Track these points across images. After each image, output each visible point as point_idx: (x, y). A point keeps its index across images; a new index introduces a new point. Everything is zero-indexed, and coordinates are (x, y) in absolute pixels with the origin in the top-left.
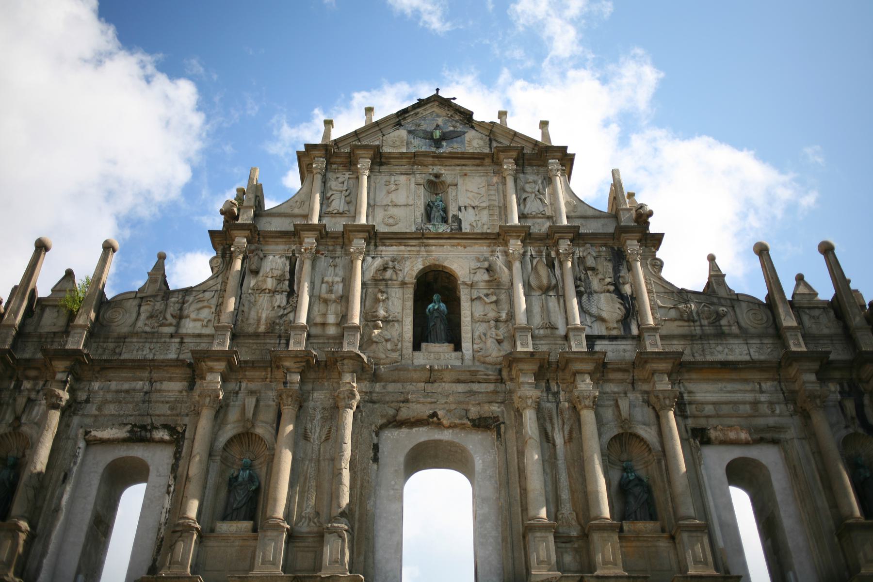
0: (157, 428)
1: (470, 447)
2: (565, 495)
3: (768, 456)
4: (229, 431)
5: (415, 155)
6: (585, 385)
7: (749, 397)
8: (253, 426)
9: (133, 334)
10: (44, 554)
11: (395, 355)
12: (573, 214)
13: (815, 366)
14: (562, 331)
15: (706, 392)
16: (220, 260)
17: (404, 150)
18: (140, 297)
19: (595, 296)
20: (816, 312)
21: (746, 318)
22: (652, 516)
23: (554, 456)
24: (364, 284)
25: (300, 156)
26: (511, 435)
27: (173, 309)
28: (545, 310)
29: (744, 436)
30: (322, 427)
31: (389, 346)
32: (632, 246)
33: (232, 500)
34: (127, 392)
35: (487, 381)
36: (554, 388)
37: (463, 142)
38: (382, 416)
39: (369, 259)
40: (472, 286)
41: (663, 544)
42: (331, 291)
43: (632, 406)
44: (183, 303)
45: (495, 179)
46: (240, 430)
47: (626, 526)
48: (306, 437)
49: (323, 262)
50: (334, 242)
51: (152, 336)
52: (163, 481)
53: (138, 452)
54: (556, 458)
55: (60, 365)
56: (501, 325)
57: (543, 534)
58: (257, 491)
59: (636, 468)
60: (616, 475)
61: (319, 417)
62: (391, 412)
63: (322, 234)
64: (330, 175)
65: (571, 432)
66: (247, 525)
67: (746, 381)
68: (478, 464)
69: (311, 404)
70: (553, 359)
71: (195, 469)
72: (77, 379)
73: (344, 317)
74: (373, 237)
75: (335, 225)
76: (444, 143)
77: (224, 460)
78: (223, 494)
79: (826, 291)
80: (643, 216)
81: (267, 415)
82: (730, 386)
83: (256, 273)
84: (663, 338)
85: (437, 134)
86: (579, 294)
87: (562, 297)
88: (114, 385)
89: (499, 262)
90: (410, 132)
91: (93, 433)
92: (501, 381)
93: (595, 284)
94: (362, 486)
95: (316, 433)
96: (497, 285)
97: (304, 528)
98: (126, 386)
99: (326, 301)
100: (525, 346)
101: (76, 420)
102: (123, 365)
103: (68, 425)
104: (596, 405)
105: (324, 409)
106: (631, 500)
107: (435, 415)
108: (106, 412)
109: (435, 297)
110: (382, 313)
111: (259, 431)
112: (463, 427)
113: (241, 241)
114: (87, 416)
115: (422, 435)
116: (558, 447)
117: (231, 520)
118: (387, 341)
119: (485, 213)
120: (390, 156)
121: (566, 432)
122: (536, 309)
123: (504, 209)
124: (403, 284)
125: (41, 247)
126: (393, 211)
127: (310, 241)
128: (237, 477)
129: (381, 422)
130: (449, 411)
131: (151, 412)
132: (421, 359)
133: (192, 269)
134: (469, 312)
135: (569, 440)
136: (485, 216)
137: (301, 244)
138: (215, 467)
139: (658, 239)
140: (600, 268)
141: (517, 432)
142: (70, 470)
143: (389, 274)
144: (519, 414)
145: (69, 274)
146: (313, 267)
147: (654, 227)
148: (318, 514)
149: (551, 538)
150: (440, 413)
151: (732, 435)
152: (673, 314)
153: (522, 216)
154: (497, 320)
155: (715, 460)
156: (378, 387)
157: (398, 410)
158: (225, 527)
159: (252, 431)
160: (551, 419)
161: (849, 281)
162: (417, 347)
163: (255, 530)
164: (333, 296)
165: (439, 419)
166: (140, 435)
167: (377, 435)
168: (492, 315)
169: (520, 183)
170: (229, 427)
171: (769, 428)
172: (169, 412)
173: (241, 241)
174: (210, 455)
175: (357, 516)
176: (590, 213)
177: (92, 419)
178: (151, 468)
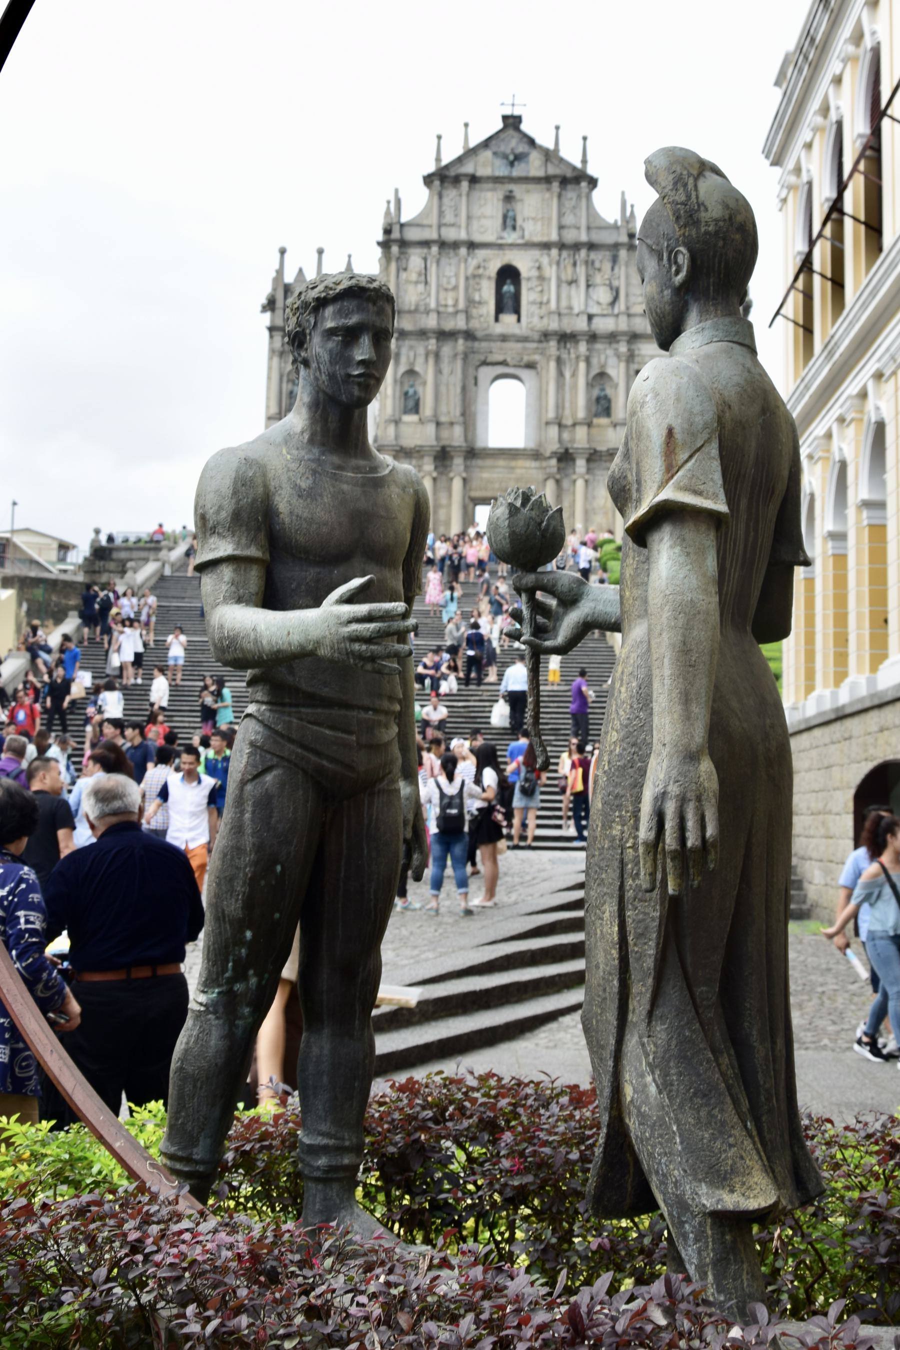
2: (567, 405)
4: (403, 369)
6: (583, 347)
11: (485, 325)
12: (592, 225)
14: (576, 311)
16: (384, 260)
19: (597, 288)
23: (564, 384)
24: (467, 278)
26: (544, 373)
28: (569, 298)
31: (482, 319)
32: (623, 253)
35: (533, 341)
36: (568, 345)
37: (527, 162)
39: (470, 259)
40: (529, 279)
42: (448, 283)
43: (607, 357)
45: (547, 195)
47: (596, 421)
49: (444, 261)
56: (544, 307)
60: (596, 392)
62: (482, 358)
63: (443, 244)
64: (445, 193)
70: (568, 331)
73: (456, 301)
74: (472, 246)
75: (450, 234)
76: (516, 163)
77: (402, 383)
83: (405, 269)
84: (629, 316)
85: (511, 157)
86: (588, 286)
87: (578, 287)
90: (495, 154)
92: (540, 341)
93: (598, 279)
97: (443, 419)
99: (446, 290)
100: (553, 325)
104: (588, 360)
109: (508, 281)
110: (477, 298)
112: (520, 366)
113: (395, 249)
115: (500, 370)
118: (481, 316)
119: (539, 223)
122: (564, 295)
123: (549, 225)
124: (489, 278)
125: (283, 252)
127: (435, 249)
134: (527, 297)
136: (539, 226)
137: (429, 248)
138: (398, 388)
140: (603, 268)
143: (481, 271)
145: (301, 270)
150: (509, 360)
153: (561, 227)
154: (541, 303)
156: (476, 344)
162: (497, 319)
164: (450, 287)
168: (539, 300)
169: (563, 198)
173: (395, 249)
174: (395, 381)
176: (603, 224)
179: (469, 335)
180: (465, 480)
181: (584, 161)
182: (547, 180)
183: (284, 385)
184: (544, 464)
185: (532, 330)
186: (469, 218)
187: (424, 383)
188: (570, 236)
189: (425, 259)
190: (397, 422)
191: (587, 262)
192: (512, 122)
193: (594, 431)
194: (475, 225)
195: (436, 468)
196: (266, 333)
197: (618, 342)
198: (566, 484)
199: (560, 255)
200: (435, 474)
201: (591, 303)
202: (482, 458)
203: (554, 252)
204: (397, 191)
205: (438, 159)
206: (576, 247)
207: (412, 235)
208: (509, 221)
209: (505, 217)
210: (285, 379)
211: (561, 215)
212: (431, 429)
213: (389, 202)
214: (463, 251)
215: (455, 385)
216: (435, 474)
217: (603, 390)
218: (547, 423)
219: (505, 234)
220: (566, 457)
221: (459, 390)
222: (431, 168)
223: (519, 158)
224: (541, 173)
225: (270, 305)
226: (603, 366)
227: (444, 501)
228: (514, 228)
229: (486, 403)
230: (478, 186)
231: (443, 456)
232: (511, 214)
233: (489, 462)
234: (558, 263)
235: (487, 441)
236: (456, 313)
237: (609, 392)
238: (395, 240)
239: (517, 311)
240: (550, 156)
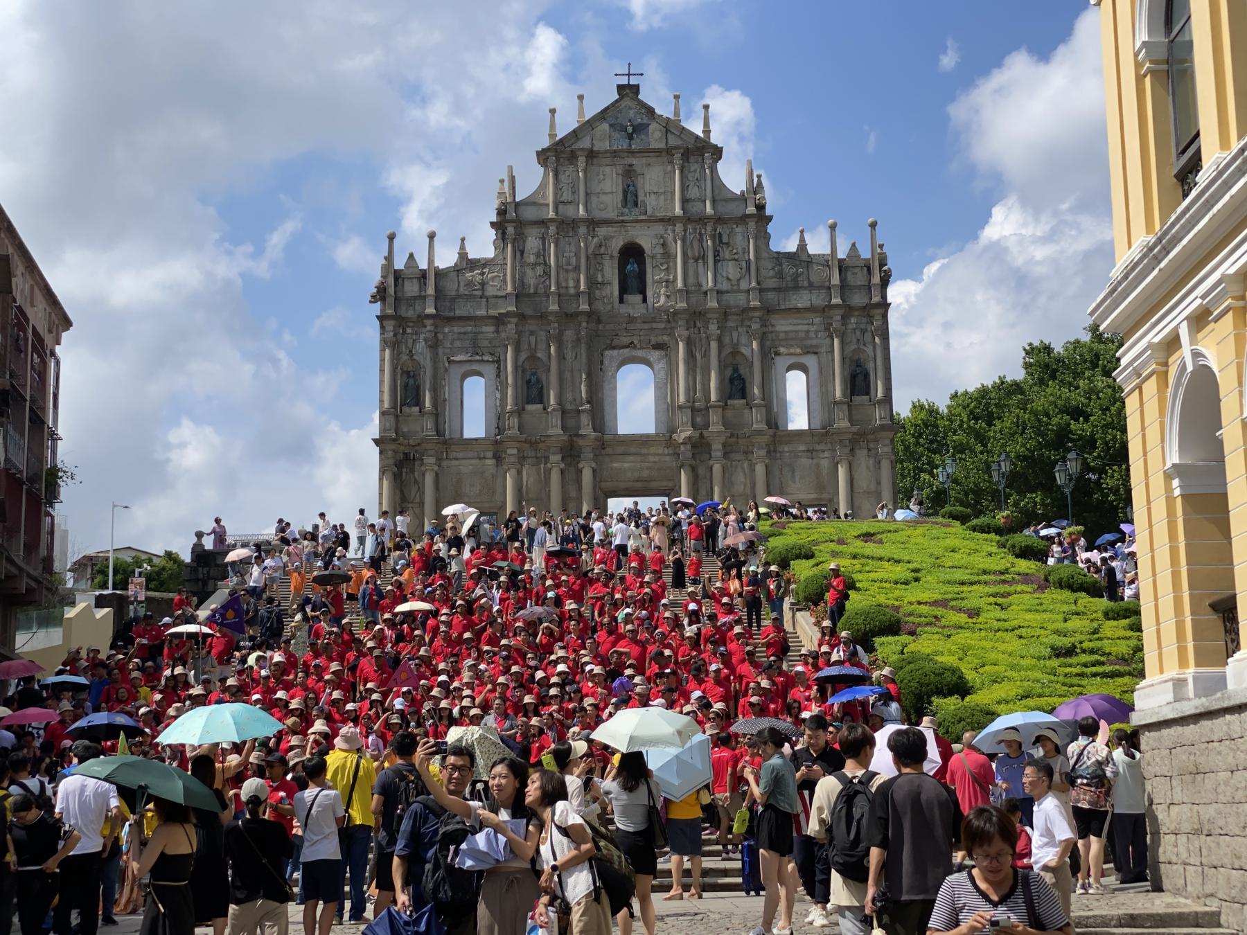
3: (811, 361)
4: (523, 356)
5: (615, 151)
6: (713, 328)
7: (806, 328)
9: (459, 296)
13: (841, 312)
14: (704, 288)
15: (782, 325)
16: (500, 242)
17: (606, 145)
18: (456, 270)
20: (857, 270)
21: (816, 275)
22: (744, 397)
24: (588, 258)
25: (538, 153)
27: (479, 278)
28: (697, 274)
29: (799, 351)
32: (752, 225)
34: (464, 333)
36: (698, 324)
37: (647, 135)
41: (747, 411)
42: (569, 264)
44: (483, 274)
45: (669, 168)
47: (729, 402)
49: (562, 242)
50: (567, 226)
51: (470, 297)
53: (476, 367)
55: (428, 322)
60: (729, 372)
64: (561, 169)
66: (540, 406)
67: (805, 318)
68: (656, 367)
69: (565, 338)
71: (510, 381)
72: (436, 327)
74: (592, 223)
77: (524, 371)
79: (865, 253)
80: (761, 208)
81: (542, 346)
82: (795, 322)
84: (761, 291)
85: (630, 130)
86: (716, 262)
88: (456, 329)
89: (670, 238)
90: (611, 126)
92: (669, 322)
95: (570, 355)
96: (668, 256)
97: (569, 407)
98: (463, 330)
99: (567, 271)
101: (440, 351)
102: (460, 318)
110: (600, 279)
111: (539, 355)
113: (510, 230)
115: (626, 352)
120: (598, 152)
126: (603, 198)
132: (624, 309)
133: (483, 245)
136: (662, 202)
139: (770, 218)
143: (602, 250)
145: (411, 255)
146: (556, 246)
147: (768, 212)
151: (792, 351)
152: (771, 273)
153: (685, 201)
155: (781, 363)
156: (601, 327)
161: (881, 246)
162: (621, 301)
171: (812, 346)
176: (729, 196)
179: (592, 315)
180: (594, 471)
181: (707, 132)
182: (669, 152)
185: (659, 309)
186: (587, 194)
187: (549, 370)
188: (695, 208)
189: (543, 239)
191: (713, 237)
192: (628, 91)
193: (729, 413)
194: (594, 201)
196: (377, 323)
197: (751, 319)
198: (702, 471)
199: (685, 230)
200: (562, 466)
201: (719, 278)
203: (679, 227)
204: (510, 168)
205: (552, 136)
206: (702, 220)
207: (529, 214)
208: (630, 197)
209: (625, 192)
211: (684, 188)
213: (502, 181)
214: (583, 230)
216: (562, 466)
217: (736, 370)
219: (626, 210)
222: (546, 143)
223: (639, 129)
224: (662, 146)
225: (381, 294)
226: (735, 346)
227: (573, 494)
228: (636, 204)
230: (595, 161)
232: (631, 188)
233: (619, 449)
234: (684, 240)
236: (578, 294)
237: (742, 371)
238: (511, 221)
239: (643, 292)
240: (671, 127)
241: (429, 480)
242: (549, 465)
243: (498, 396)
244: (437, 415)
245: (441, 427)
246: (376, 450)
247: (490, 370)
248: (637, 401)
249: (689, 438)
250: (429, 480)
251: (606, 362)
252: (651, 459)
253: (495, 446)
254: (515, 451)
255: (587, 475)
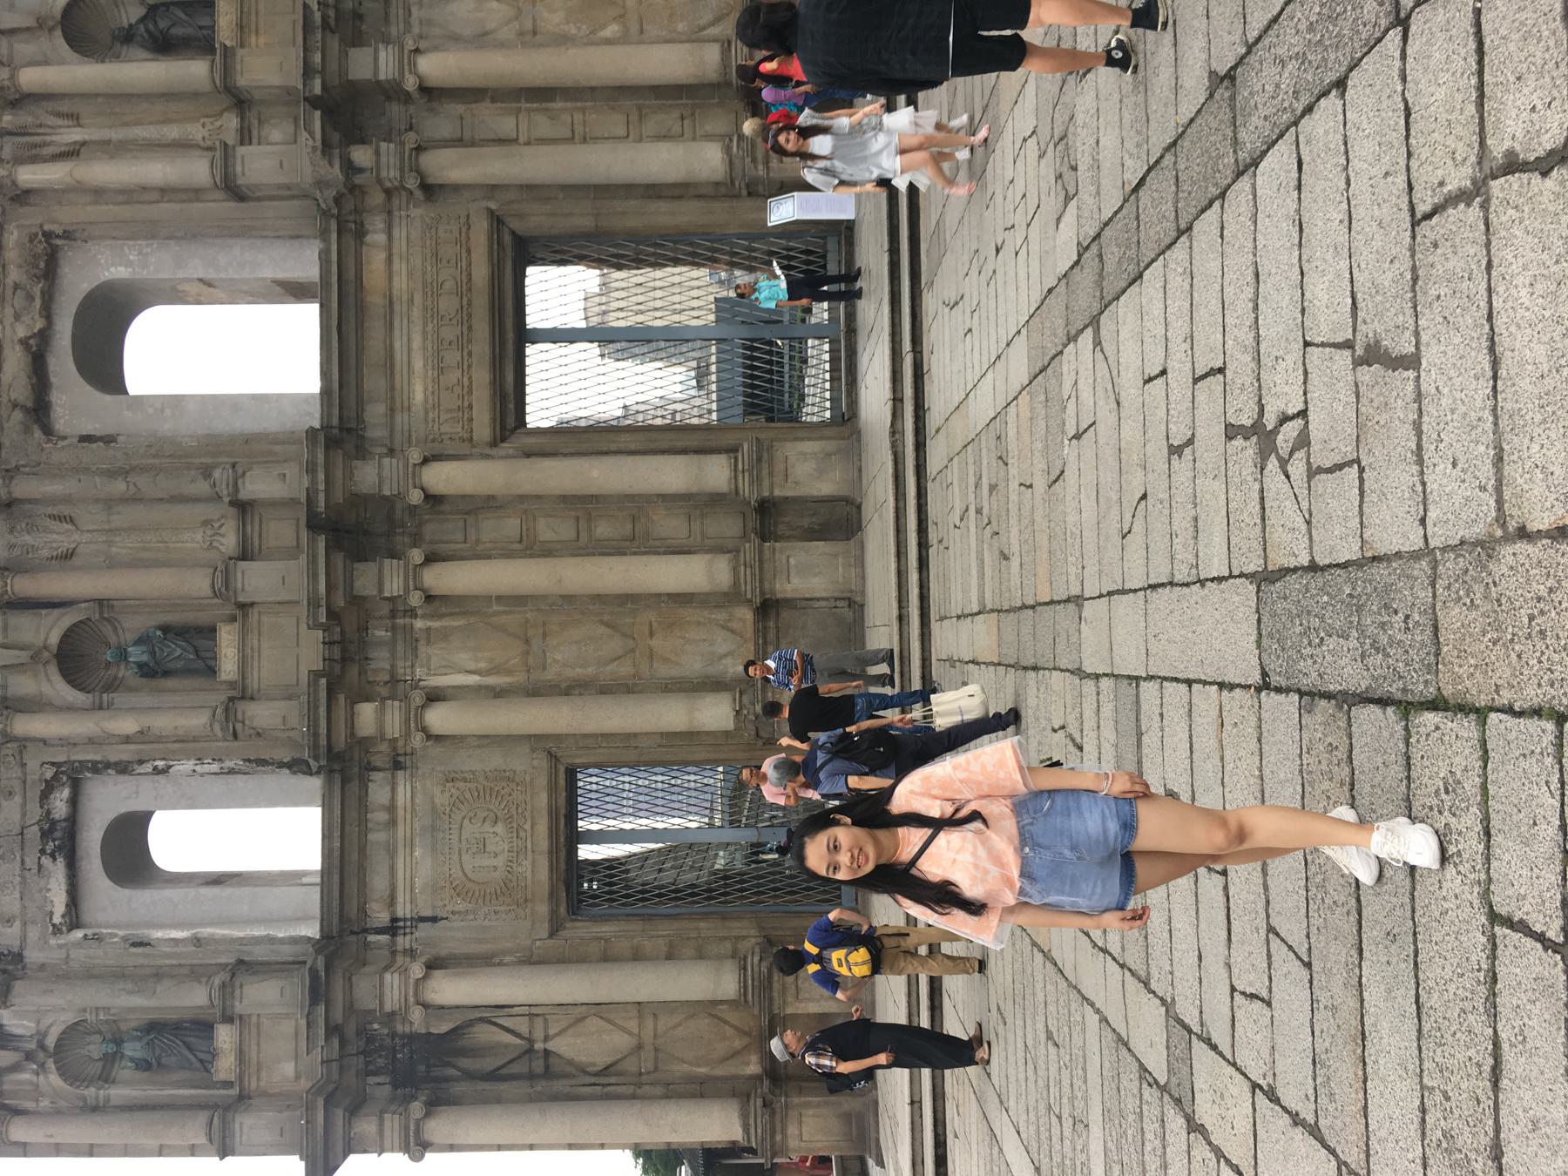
0: (49, 812)
1: (86, 287)
2: (172, 132)
4: (57, 687)
8: (45, 647)
10: (272, 940)
26: (64, 216)
30: (46, 530)
33: (180, 665)
38: (27, 430)
46: (53, 669)
48: (69, 555)
52: (147, 784)
54: (108, 142)
57: (239, 161)
58: (166, 629)
59: (126, 24)
61: (28, 539)
62: (18, 415)
65: (60, 115)
68: (119, 272)
71: (127, 725)
77: (111, 687)
78: (170, 683)
91: (57, 919)
94: (155, 456)
95: (59, 538)
97: (229, 542)
103: (42, 967)
105: (12, 530)
106: (178, 31)
107: (24, 342)
108: (16, 908)
111: (54, 639)
114: (24, 938)
115: (62, 363)
116: (87, 137)
117: (215, 659)
121: (60, 122)
128: (140, 665)
129: (38, 433)
130: (17, 317)
131: (17, 830)
135: (75, 119)
141: (60, 203)
142: (125, 939)
144: (24, 196)
148: (206, 523)
149: (241, 150)
150: (22, 332)
157: (15, 405)
158: (228, 666)
159: (54, 649)
160: (35, 146)
163: (233, 619)
165: (33, 336)
166: (62, 839)
167: (65, 438)
170: (46, 689)
172: (18, 799)
175: (209, 460)
177: (30, 928)
178: (123, 811)
183: (118, 1093)
184: (376, 198)
187: (100, 602)
190: (242, 693)
195: (394, 555)
202: (360, 403)
210: (90, 1092)
212: (257, 579)
215: (109, 503)
216: (417, 556)
218: (233, 190)
220: (345, 112)
221: (119, 486)
229: (176, 401)
231: (352, 530)
233: (374, 383)
235: (306, 398)
241: (451, 990)
242: (415, 599)
243: (187, 766)
244: (241, 962)
245: (287, 949)
246: (352, 1158)
247: (106, 801)
248: (228, 351)
249: (326, 145)
250: (451, 990)
251: (90, 428)
252: (400, 284)
253: (343, 770)
254: (367, 711)
255: (445, 477)
